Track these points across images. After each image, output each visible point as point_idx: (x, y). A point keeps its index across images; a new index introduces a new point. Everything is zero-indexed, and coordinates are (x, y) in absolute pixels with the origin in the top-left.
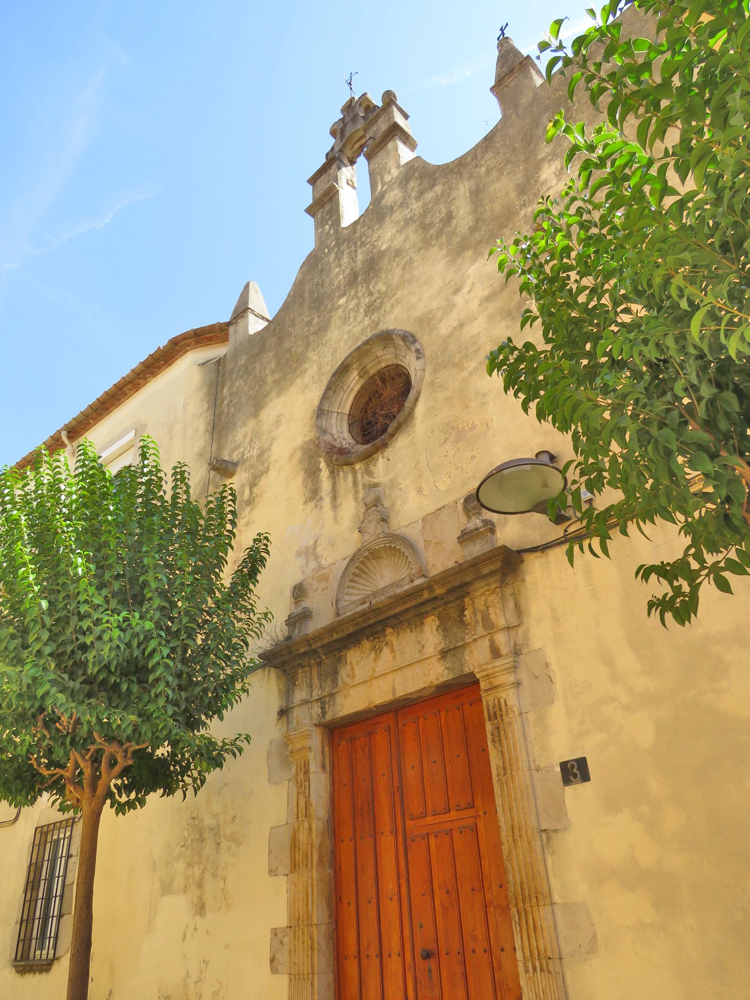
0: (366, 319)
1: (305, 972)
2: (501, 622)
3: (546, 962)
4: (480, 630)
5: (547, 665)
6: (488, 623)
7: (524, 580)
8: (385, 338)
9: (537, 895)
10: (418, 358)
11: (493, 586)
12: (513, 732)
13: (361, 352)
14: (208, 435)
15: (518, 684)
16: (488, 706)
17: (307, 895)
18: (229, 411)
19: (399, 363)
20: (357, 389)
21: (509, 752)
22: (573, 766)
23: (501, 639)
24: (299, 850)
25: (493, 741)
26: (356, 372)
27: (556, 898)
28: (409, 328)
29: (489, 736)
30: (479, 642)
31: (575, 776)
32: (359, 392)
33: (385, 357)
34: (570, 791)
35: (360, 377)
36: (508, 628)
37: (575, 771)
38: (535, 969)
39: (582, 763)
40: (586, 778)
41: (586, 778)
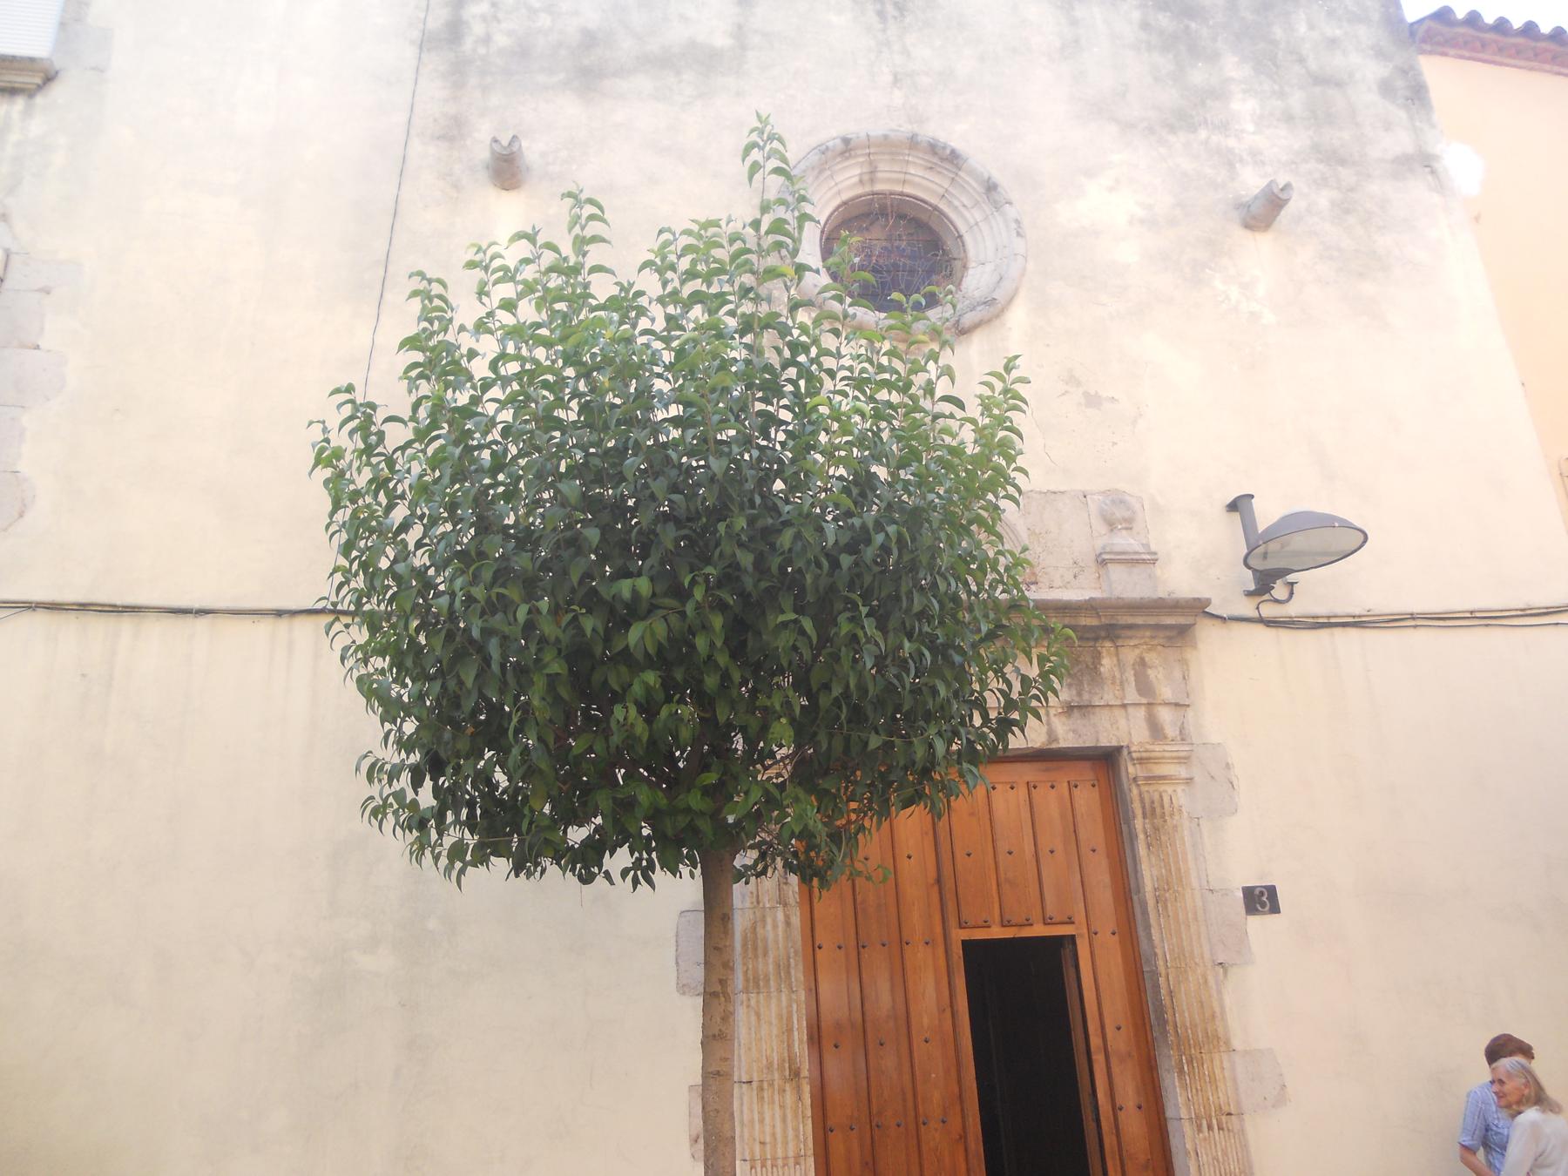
0: (897, 93)
1: (791, 1154)
2: (1166, 692)
3: (1222, 1119)
4: (1132, 695)
5: (1228, 766)
6: (1144, 687)
7: (1194, 646)
8: (947, 158)
9: (1216, 1040)
10: (1018, 234)
11: (1156, 642)
12: (1183, 839)
13: (889, 147)
14: (410, 53)
15: (1189, 781)
16: (1142, 800)
17: (790, 1031)
18: (487, 40)
19: (943, 206)
20: (845, 196)
21: (1177, 862)
22: (1262, 894)
23: (1165, 715)
24: (765, 954)
25: (1149, 846)
26: (857, 171)
27: (1236, 1043)
28: (997, 177)
29: (1141, 836)
30: (1130, 710)
31: (1263, 905)
32: (845, 203)
33: (923, 184)
34: (1254, 921)
35: (861, 181)
36: (1177, 705)
37: (1261, 900)
38: (1210, 1127)
39: (1272, 891)
40: (1275, 909)
41: (1275, 909)
